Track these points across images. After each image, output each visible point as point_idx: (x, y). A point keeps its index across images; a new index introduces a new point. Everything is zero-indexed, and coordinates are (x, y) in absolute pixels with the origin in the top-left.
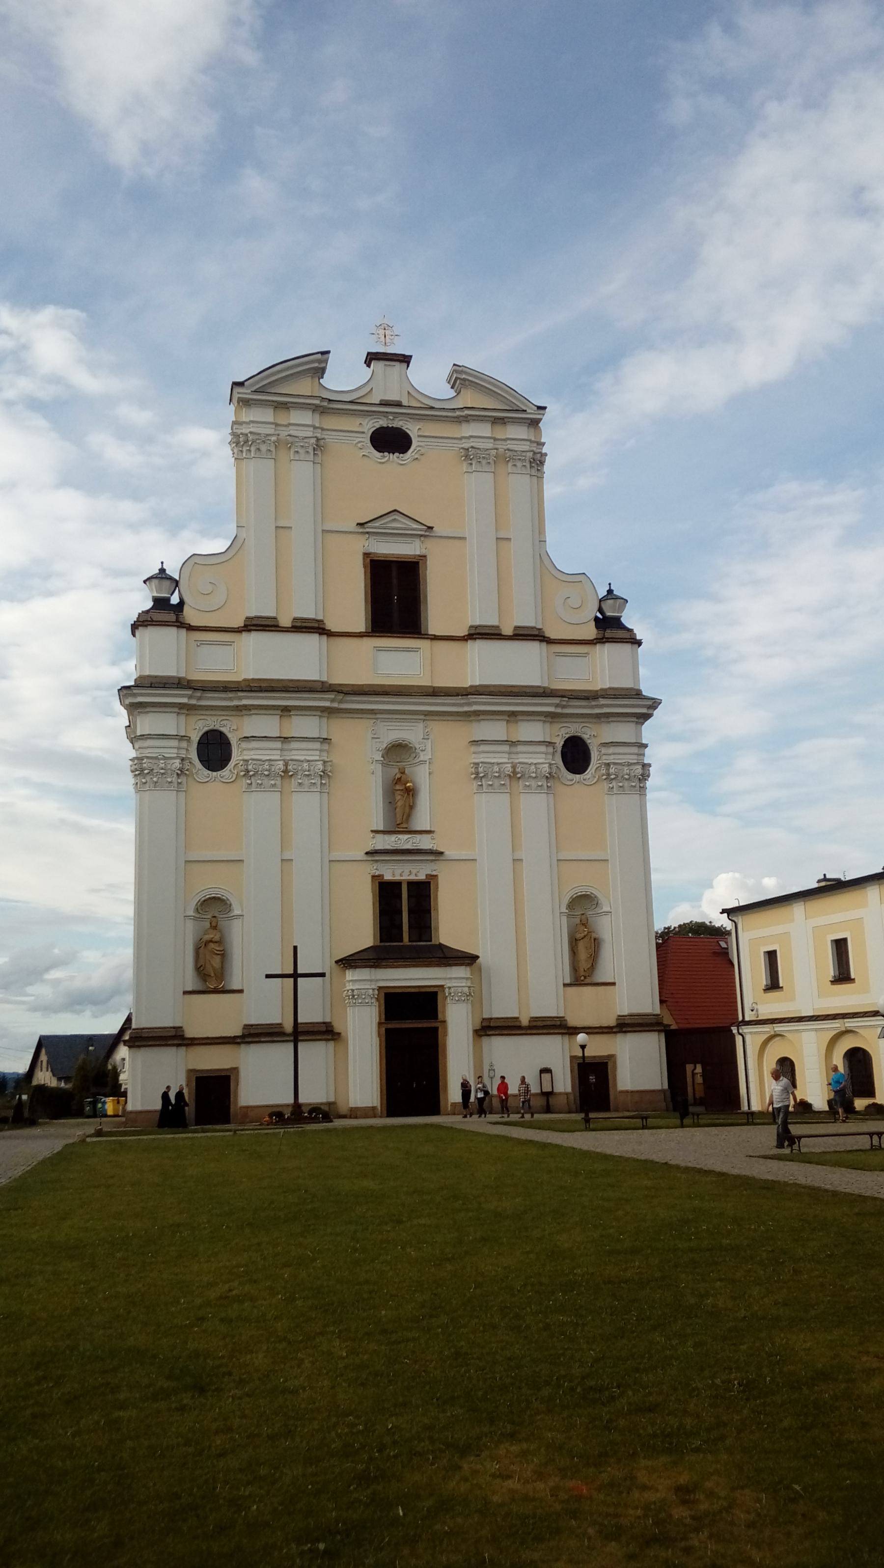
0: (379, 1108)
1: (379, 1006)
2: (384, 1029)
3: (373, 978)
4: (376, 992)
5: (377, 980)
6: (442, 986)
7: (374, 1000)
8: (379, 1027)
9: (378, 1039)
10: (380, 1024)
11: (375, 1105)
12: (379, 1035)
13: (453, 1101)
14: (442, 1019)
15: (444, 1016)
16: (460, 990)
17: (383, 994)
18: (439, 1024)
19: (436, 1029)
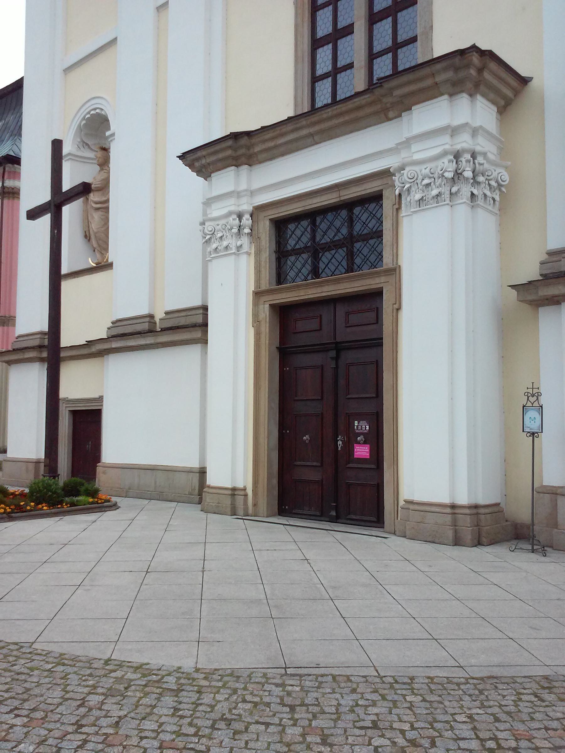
0: (250, 492)
1: (258, 253)
2: (267, 306)
3: (243, 186)
4: (247, 220)
5: (252, 193)
6: (386, 174)
7: (245, 241)
8: (256, 304)
9: (252, 332)
10: (258, 294)
11: (240, 485)
12: (256, 321)
13: (406, 498)
14: (391, 266)
15: (396, 256)
16: (424, 170)
17: (268, 223)
18: (383, 279)
19: (378, 294)
